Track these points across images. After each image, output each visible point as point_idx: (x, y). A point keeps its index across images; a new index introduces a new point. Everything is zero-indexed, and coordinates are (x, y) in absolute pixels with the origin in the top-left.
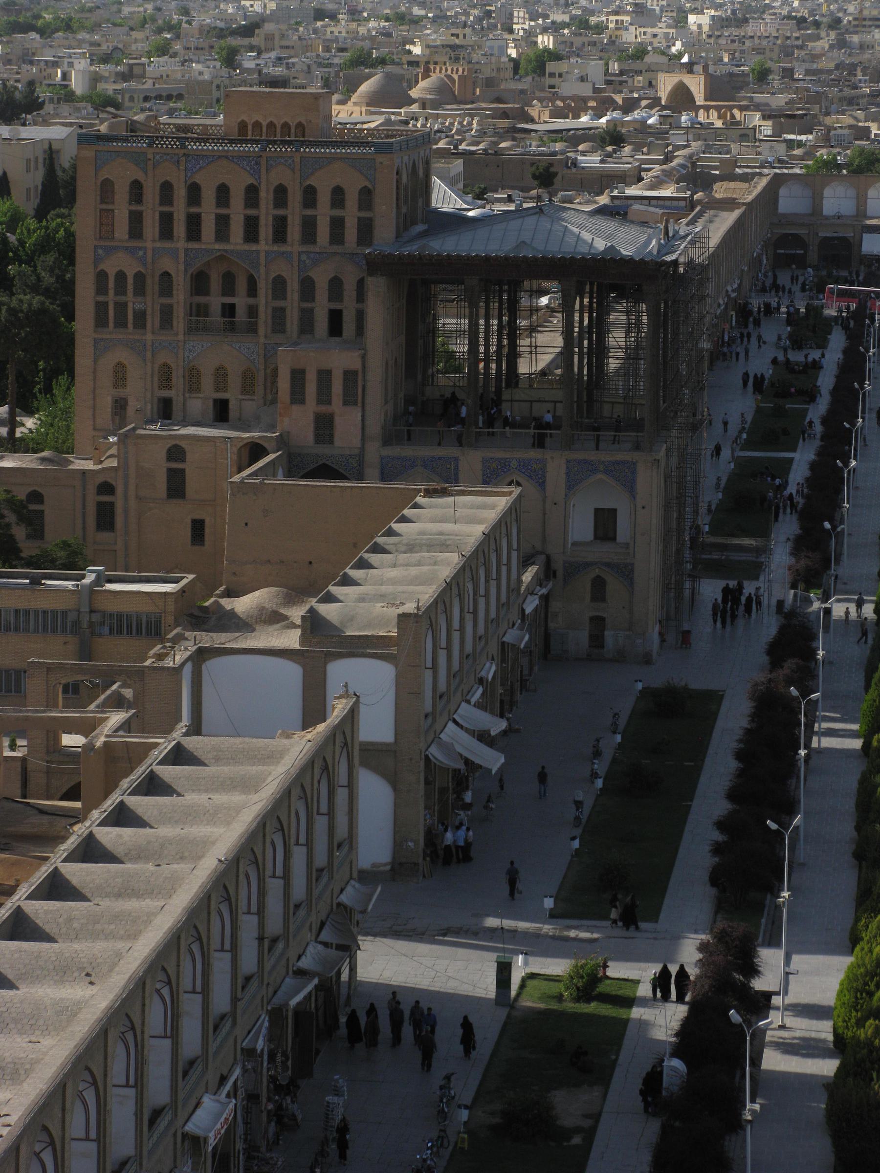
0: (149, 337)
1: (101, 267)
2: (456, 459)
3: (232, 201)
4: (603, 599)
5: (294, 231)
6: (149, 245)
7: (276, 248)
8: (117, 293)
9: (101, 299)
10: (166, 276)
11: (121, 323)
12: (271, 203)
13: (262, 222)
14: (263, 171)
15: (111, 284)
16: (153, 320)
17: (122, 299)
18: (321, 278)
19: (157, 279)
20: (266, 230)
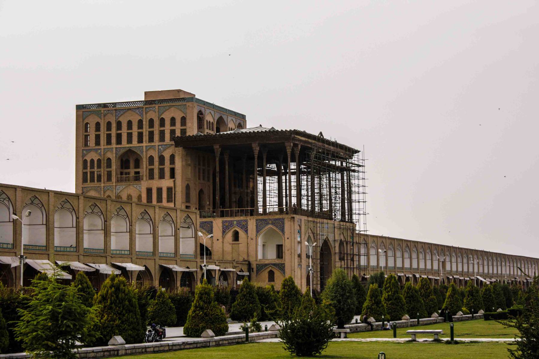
0: (102, 185)
1: (85, 158)
2: (212, 222)
3: (133, 127)
4: (273, 281)
5: (156, 137)
6: (102, 147)
7: (149, 144)
8: (90, 169)
9: (85, 171)
10: (109, 160)
11: (92, 180)
12: (148, 127)
13: (144, 134)
14: (144, 114)
15: (89, 165)
16: (104, 178)
17: (93, 170)
18: (167, 155)
19: (105, 161)
20: (146, 138)
